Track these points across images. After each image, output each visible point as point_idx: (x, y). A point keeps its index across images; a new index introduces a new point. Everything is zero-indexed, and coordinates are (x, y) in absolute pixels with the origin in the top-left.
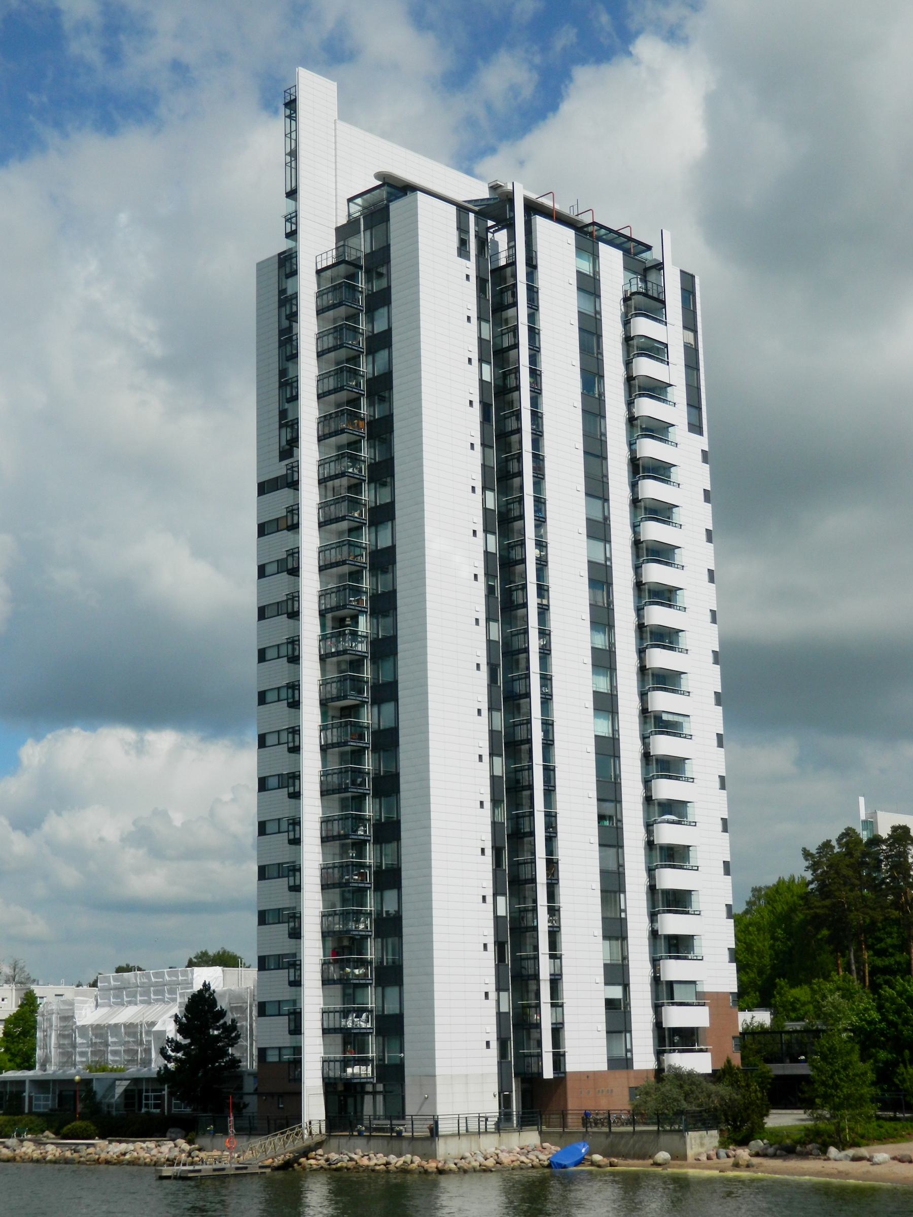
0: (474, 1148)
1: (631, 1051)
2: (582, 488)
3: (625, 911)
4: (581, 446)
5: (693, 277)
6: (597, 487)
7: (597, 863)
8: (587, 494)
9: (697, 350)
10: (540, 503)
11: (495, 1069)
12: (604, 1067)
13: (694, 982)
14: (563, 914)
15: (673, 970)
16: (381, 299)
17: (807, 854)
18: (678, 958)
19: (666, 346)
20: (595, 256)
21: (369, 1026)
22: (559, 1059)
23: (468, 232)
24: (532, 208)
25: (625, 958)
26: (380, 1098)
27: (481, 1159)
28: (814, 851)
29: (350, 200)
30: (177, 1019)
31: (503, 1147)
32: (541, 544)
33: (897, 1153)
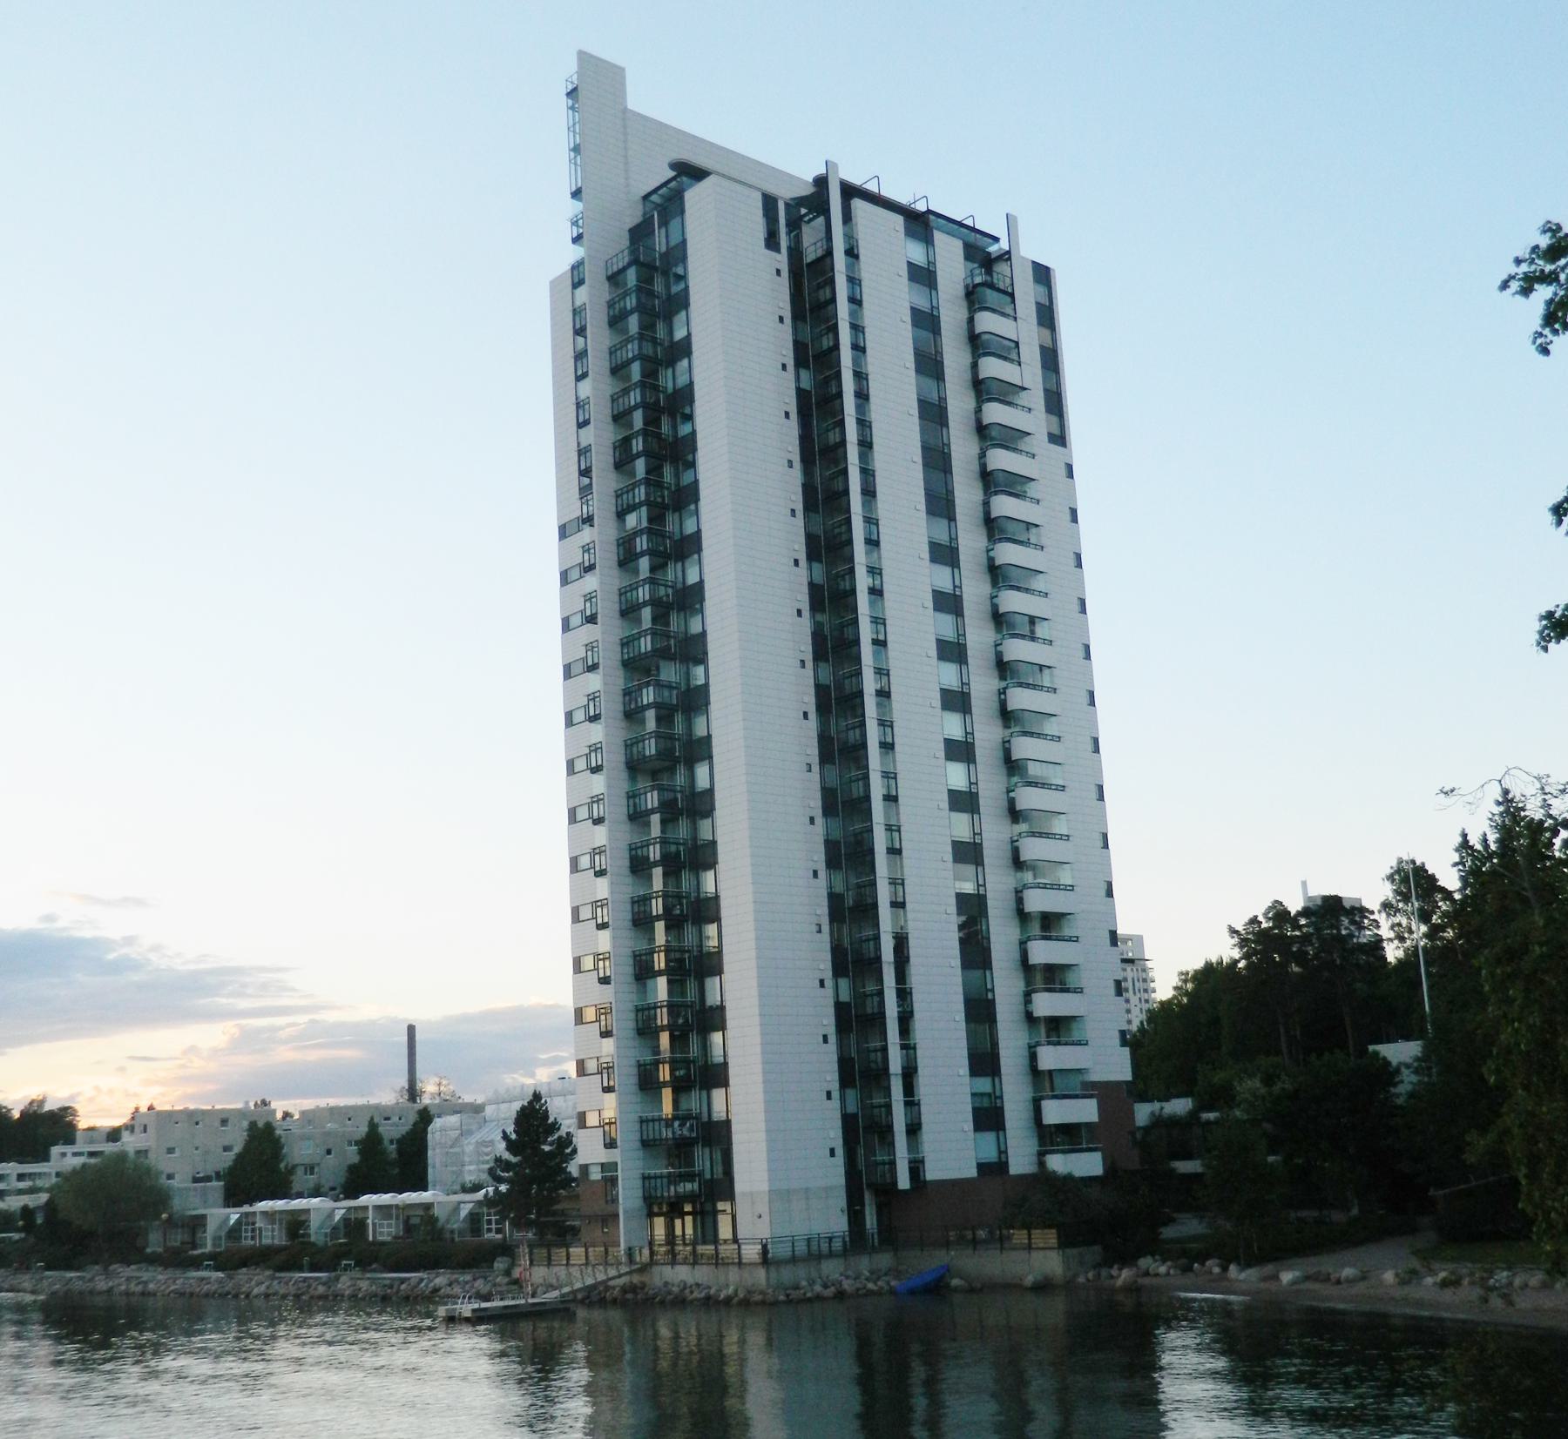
0: (814, 1274)
3: (992, 990)
4: (918, 458)
6: (940, 504)
12: (973, 1173)
13: (1079, 1070)
14: (915, 997)
17: (1233, 932)
18: (1059, 1043)
19: (1017, 344)
22: (916, 1168)
23: (777, 220)
24: (850, 192)
25: (995, 1044)
26: (689, 1219)
27: (818, 1288)
28: (1240, 928)
29: (646, 197)
30: (505, 1136)
31: (850, 1273)
33: (1312, 1270)
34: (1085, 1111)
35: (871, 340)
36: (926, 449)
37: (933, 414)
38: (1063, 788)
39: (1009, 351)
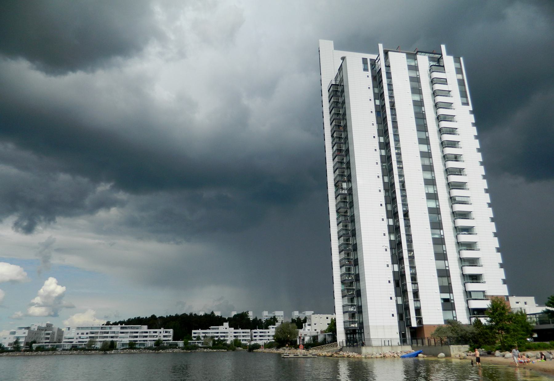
1: (456, 317)
3: (448, 267)
5: (459, 58)
7: (433, 250)
8: (418, 131)
9: (463, 80)
10: (396, 135)
11: (397, 324)
12: (442, 323)
13: (484, 292)
15: (471, 287)
16: (343, 91)
20: (416, 59)
21: (355, 310)
25: (450, 283)
32: (398, 148)
34: (485, 304)
35: (395, 87)
36: (416, 113)
37: (419, 105)
39: (444, 82)
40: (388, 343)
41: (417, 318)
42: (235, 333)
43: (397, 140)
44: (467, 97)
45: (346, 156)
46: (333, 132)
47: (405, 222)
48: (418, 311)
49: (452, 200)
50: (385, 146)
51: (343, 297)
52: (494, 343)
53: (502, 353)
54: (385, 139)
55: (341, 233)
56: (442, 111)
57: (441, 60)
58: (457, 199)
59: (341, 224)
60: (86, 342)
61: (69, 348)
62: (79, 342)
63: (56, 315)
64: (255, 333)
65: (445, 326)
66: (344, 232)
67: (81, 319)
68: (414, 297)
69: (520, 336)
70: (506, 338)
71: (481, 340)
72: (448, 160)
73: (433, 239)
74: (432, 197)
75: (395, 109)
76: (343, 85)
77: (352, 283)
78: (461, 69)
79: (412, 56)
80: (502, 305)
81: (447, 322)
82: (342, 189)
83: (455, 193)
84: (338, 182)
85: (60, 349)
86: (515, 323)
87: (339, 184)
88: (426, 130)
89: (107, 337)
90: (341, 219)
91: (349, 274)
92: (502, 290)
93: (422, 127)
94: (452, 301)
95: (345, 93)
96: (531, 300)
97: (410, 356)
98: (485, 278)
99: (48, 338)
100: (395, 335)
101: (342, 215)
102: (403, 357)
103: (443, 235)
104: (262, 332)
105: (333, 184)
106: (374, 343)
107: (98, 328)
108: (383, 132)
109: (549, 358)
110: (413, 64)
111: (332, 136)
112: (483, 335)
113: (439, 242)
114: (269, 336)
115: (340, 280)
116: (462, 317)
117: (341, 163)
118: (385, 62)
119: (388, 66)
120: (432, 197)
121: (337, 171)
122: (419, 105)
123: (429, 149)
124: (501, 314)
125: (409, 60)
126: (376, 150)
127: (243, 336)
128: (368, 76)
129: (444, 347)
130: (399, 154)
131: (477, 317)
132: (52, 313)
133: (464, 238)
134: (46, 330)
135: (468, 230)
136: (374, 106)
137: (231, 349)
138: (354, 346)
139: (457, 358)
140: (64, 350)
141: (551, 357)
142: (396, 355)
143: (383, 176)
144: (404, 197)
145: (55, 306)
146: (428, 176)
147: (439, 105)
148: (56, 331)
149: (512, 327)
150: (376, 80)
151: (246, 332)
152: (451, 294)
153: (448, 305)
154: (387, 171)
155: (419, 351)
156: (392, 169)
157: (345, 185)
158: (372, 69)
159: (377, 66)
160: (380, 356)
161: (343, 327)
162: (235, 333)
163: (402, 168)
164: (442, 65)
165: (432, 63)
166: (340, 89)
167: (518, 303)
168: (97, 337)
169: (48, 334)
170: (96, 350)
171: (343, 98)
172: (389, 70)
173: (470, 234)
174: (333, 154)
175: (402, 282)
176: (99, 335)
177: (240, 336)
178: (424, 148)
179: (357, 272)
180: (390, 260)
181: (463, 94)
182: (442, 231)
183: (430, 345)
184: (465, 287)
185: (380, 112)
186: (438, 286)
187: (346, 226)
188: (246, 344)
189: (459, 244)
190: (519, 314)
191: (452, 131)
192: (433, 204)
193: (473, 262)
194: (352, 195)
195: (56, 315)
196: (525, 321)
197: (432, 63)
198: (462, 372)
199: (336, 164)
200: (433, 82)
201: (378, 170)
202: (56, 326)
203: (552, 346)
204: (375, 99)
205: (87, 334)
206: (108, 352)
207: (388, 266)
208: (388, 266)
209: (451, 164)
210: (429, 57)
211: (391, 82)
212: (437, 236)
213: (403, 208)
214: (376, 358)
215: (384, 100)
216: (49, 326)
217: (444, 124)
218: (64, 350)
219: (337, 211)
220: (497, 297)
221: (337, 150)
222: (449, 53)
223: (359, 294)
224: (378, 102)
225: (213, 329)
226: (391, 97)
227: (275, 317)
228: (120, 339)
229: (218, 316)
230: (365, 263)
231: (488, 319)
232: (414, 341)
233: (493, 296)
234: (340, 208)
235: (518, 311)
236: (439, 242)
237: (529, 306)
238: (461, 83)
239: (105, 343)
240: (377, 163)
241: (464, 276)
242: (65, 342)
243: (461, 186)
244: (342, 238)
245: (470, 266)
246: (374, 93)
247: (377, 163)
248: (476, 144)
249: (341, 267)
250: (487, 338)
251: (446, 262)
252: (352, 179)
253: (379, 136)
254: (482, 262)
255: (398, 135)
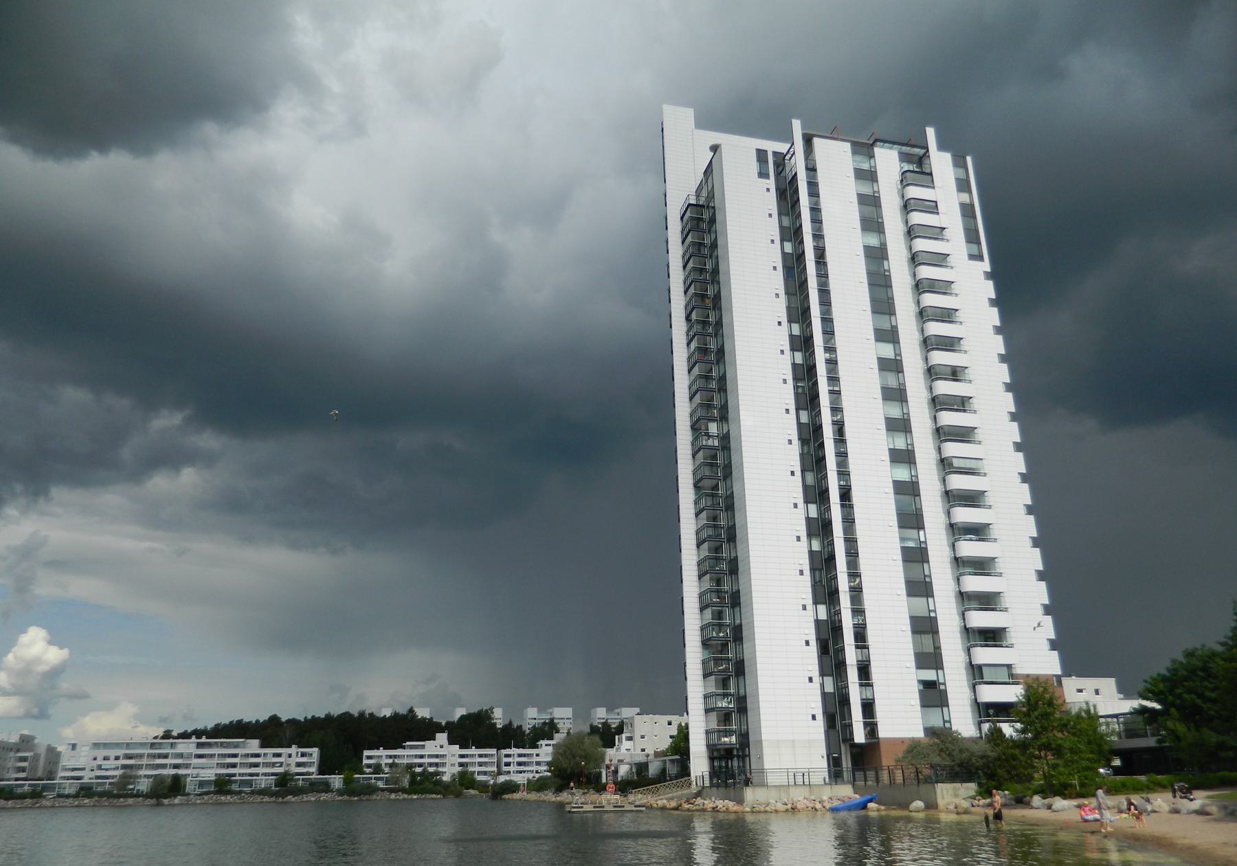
2: (869, 309)
4: (866, 281)
7: (902, 575)
8: (873, 312)
9: (972, 205)
10: (827, 321)
11: (822, 736)
13: (1009, 666)
15: (984, 655)
16: (713, 220)
20: (872, 156)
21: (731, 706)
22: (871, 728)
25: (938, 648)
32: (830, 349)
34: (1011, 694)
36: (870, 274)
37: (876, 256)
38: (985, 475)
39: (932, 207)
40: (802, 780)
41: (866, 724)
42: (462, 756)
43: (829, 332)
44: (979, 243)
45: (718, 363)
46: (689, 308)
47: (843, 512)
48: (868, 708)
49: (946, 465)
50: (803, 343)
51: (705, 676)
52: (1030, 778)
53: (1047, 801)
54: (802, 330)
55: (704, 535)
56: (926, 272)
57: (926, 161)
58: (956, 463)
59: (704, 514)
60: (113, 777)
61: (72, 791)
62: (98, 777)
63: (42, 715)
64: (507, 756)
65: (927, 740)
66: (711, 532)
67: (103, 726)
68: (860, 678)
69: (1085, 763)
70: (1055, 767)
71: (1001, 772)
72: (937, 379)
73: (904, 549)
74: (903, 457)
75: (825, 264)
76: (714, 208)
77: (725, 645)
78: (968, 181)
79: (864, 149)
80: (1047, 696)
81: (930, 731)
82: (708, 436)
83: (951, 449)
84: (699, 420)
85: (50, 795)
86: (1074, 734)
87: (702, 424)
88: (891, 312)
89: (164, 766)
90: (703, 503)
91: (720, 625)
92: (1048, 664)
93: (882, 304)
94: (942, 687)
95: (718, 226)
96: (1108, 685)
97: (849, 808)
98: (1012, 637)
99: (23, 770)
100: (816, 760)
101: (707, 495)
102: (834, 810)
103: (925, 542)
104: (524, 755)
105: (689, 424)
106: (772, 779)
107: (142, 745)
108: (798, 313)
109: (1146, 811)
110: (865, 166)
111: (688, 318)
112: (1007, 760)
113: (915, 556)
114: (538, 763)
115: (698, 639)
116: (963, 722)
117: (707, 378)
118: (806, 159)
119: (811, 169)
120: (903, 457)
121: (698, 396)
122: (876, 256)
123: (898, 353)
124: (1046, 716)
125: (859, 158)
126: (782, 352)
127: (481, 764)
128: (768, 190)
129: (924, 788)
130: (832, 363)
131: (994, 722)
132: (35, 711)
133: (969, 548)
134: (18, 751)
135: (978, 532)
136: (780, 255)
137: (452, 793)
138: (727, 786)
139: (951, 812)
140: (60, 796)
141: (1149, 808)
142: (818, 806)
143: (797, 410)
144: (842, 456)
145: (42, 692)
146: (895, 412)
147: (919, 259)
148: (42, 751)
149: (1067, 745)
150: (786, 199)
151: (486, 756)
152: (940, 672)
153: (933, 695)
154: (807, 399)
155: (869, 797)
156: (817, 396)
157: (713, 428)
158: (778, 174)
159: (788, 169)
160: (783, 808)
161: (704, 742)
162: (462, 756)
163: (839, 393)
164: (928, 171)
165: (906, 167)
166: (706, 216)
167: (1080, 691)
168: (140, 767)
169: (24, 759)
170: (137, 796)
171: (713, 236)
172: (815, 177)
173: (983, 540)
174: (689, 358)
175: (835, 643)
176: (145, 761)
177: (473, 764)
178: (887, 351)
179: (738, 622)
180: (810, 596)
181: (971, 236)
182: (921, 533)
183: (892, 782)
184: (970, 655)
185: (793, 267)
186: (912, 652)
187: (715, 518)
188: (486, 782)
189: (958, 562)
190: (1083, 714)
191: (947, 315)
192: (903, 474)
193: (988, 601)
194: (729, 449)
195: (42, 715)
196: (1095, 731)
197: (906, 167)
198: (960, 845)
199: (695, 380)
200: (907, 207)
201: (787, 395)
202: (42, 741)
203: (1151, 785)
204: (782, 240)
205: (117, 758)
206: (166, 801)
207: (804, 608)
208: (804, 608)
209: (944, 388)
210: (900, 153)
211: (817, 203)
212: (911, 544)
213: (839, 480)
214: (776, 811)
215: (802, 242)
216: (26, 742)
217: (930, 300)
218: (60, 796)
219: (697, 486)
220: (1037, 678)
221: (698, 349)
222: (942, 147)
223: (740, 669)
224: (788, 247)
225: (412, 747)
226: (818, 236)
227: (552, 720)
228: (195, 772)
229: (424, 719)
230: (754, 600)
231: (1018, 726)
232: (859, 775)
233: (1028, 676)
234: (701, 479)
235: (1081, 709)
236: (915, 556)
237: (1104, 699)
238: (967, 211)
239: (158, 780)
240: (785, 381)
241: (967, 631)
242: (64, 778)
243: (964, 435)
244: (706, 545)
245: (981, 609)
246: (782, 228)
247: (785, 381)
248: (998, 345)
249: (702, 609)
250: (1014, 767)
251: (930, 600)
252: (731, 415)
253: (790, 321)
254: (1006, 601)
255: (831, 321)
